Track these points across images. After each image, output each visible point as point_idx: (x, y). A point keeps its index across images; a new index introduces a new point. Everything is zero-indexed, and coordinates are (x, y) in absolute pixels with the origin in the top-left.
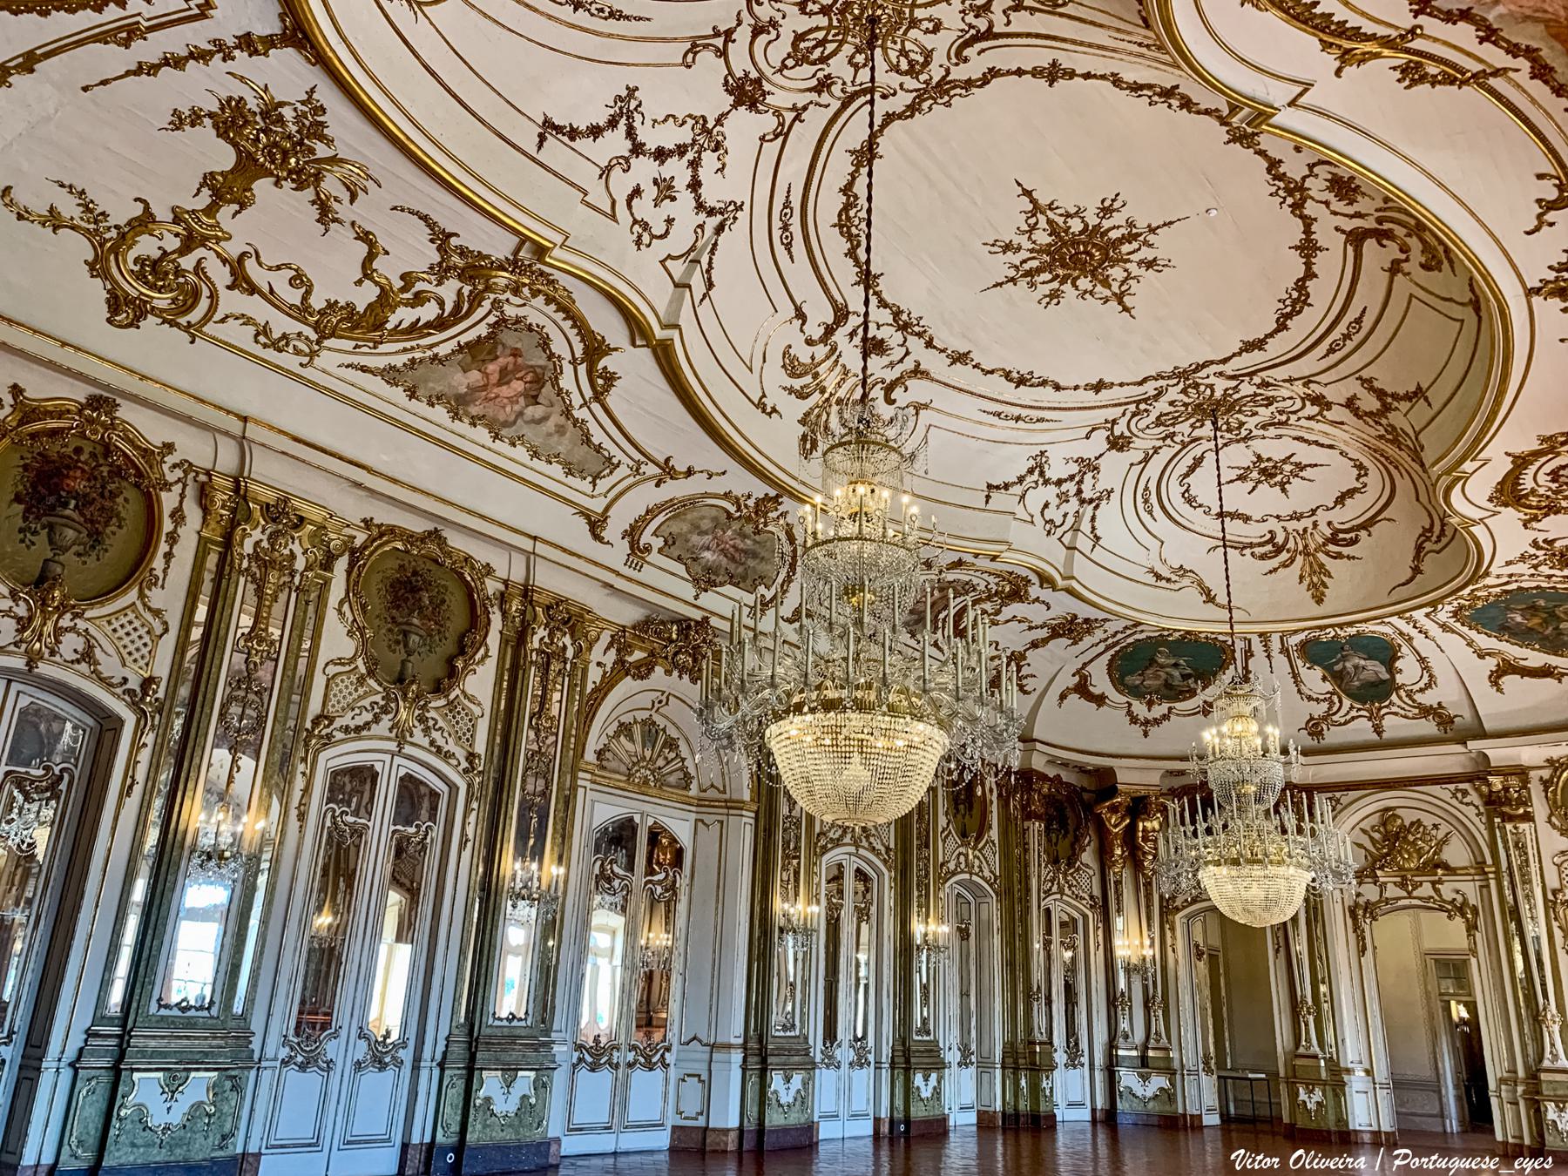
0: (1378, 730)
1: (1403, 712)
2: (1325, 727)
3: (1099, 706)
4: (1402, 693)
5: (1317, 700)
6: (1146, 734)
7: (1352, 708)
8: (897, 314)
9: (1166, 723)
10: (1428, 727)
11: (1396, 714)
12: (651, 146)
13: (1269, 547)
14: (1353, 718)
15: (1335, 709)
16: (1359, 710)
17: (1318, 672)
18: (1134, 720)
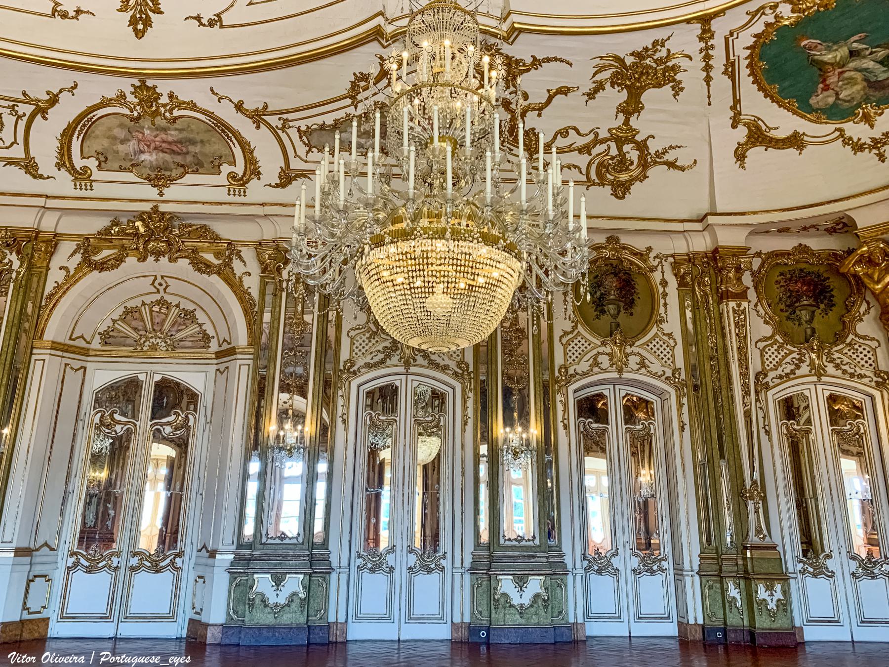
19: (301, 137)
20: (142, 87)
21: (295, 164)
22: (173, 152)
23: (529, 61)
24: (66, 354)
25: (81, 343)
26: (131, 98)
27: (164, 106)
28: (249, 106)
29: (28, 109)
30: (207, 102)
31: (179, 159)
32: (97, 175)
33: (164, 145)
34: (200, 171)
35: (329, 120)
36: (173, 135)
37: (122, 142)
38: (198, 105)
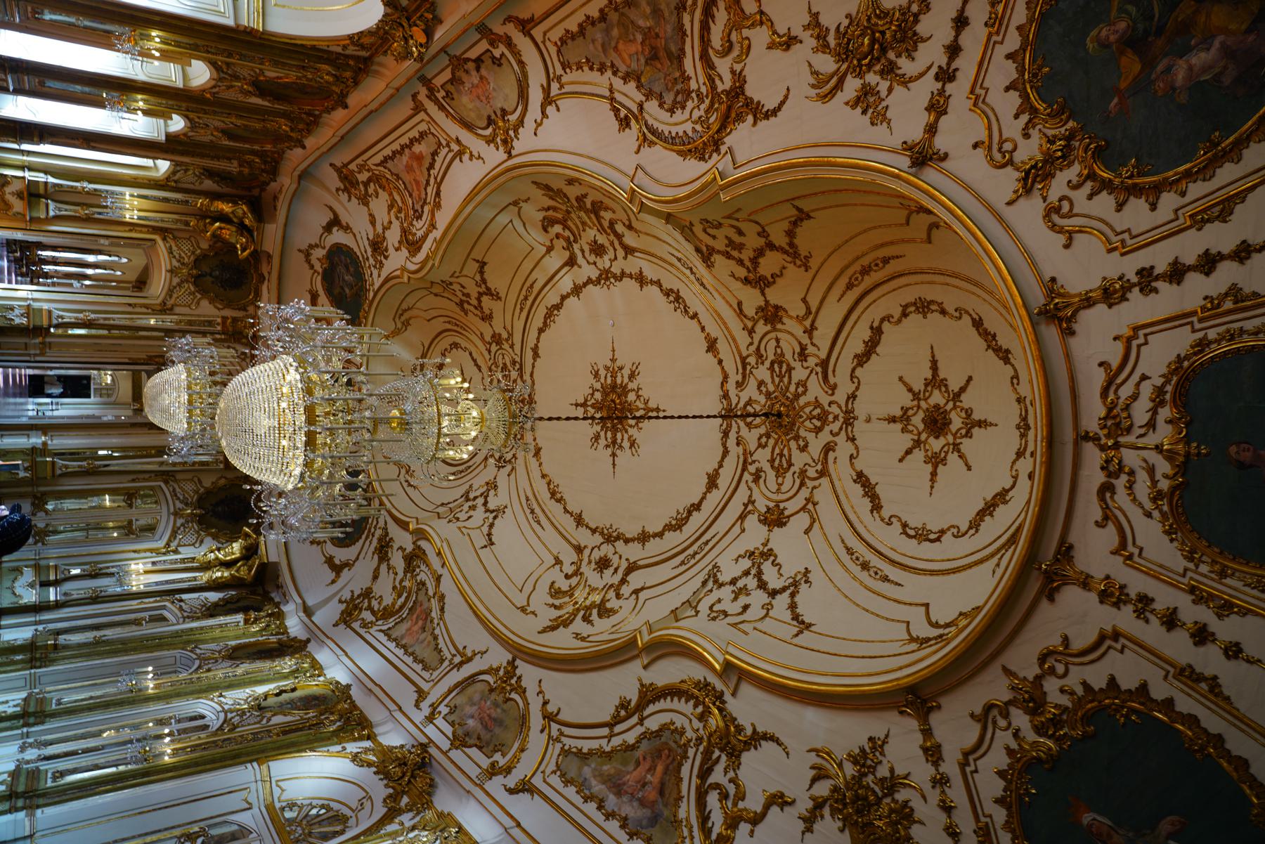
6: (300, 251)
8: (615, 277)
9: (307, 266)
12: (768, 253)
18: (311, 246)
19: (559, 755)
20: (511, 663)
21: (537, 781)
22: (486, 727)
23: (749, 731)
24: (260, 783)
25: (277, 791)
26: (501, 673)
27: (511, 685)
28: (551, 708)
29: (457, 659)
30: (531, 694)
31: (483, 733)
32: (439, 721)
33: (487, 718)
34: (484, 750)
35: (586, 746)
36: (496, 713)
37: (473, 704)
38: (527, 694)
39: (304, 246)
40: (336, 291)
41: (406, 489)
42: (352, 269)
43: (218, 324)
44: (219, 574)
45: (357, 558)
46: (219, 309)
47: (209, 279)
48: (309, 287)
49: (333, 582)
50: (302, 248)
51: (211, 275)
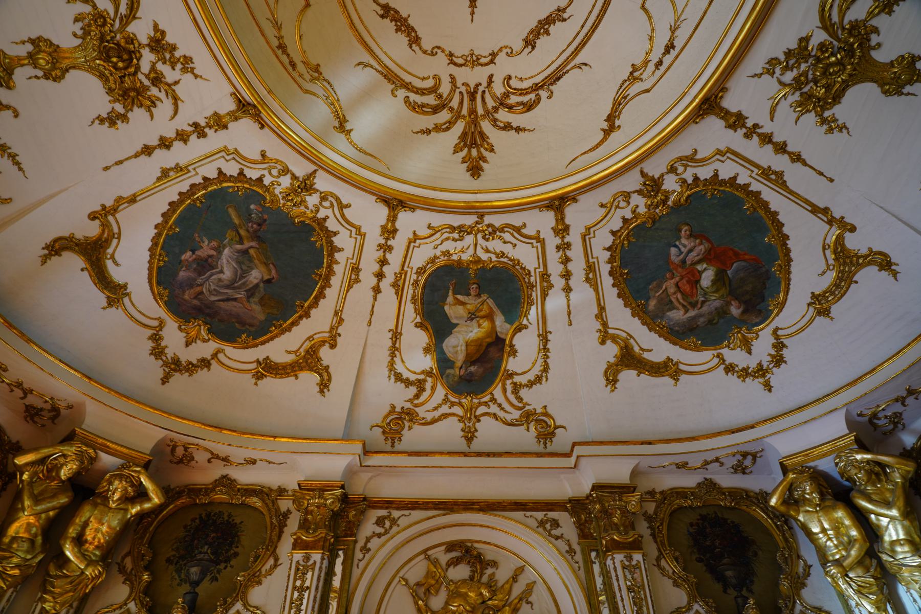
0: (469, 436)
1: (501, 414)
2: (407, 424)
3: (111, 303)
4: (509, 388)
5: (408, 383)
6: (165, 380)
7: (446, 400)
9: (202, 374)
10: (526, 437)
11: (495, 416)
13: (431, 100)
14: (445, 416)
15: (421, 399)
16: (453, 404)
17: (422, 338)
18: (158, 352)
39: (156, 368)
40: (257, 312)
41: (677, 49)
42: (206, 249)
43: (307, 558)
44: (903, 551)
45: (826, 211)
46: (276, 566)
47: (204, 589)
48: (248, 378)
49: (886, 264)
50: (161, 374)
51: (197, 583)
